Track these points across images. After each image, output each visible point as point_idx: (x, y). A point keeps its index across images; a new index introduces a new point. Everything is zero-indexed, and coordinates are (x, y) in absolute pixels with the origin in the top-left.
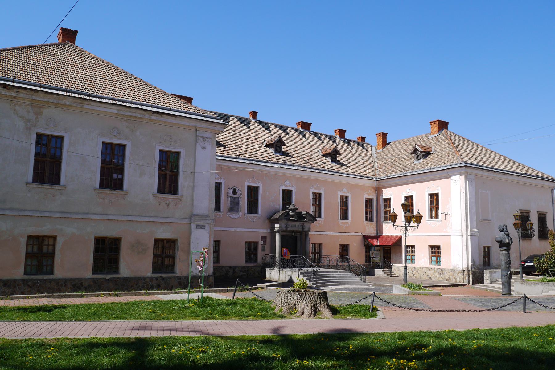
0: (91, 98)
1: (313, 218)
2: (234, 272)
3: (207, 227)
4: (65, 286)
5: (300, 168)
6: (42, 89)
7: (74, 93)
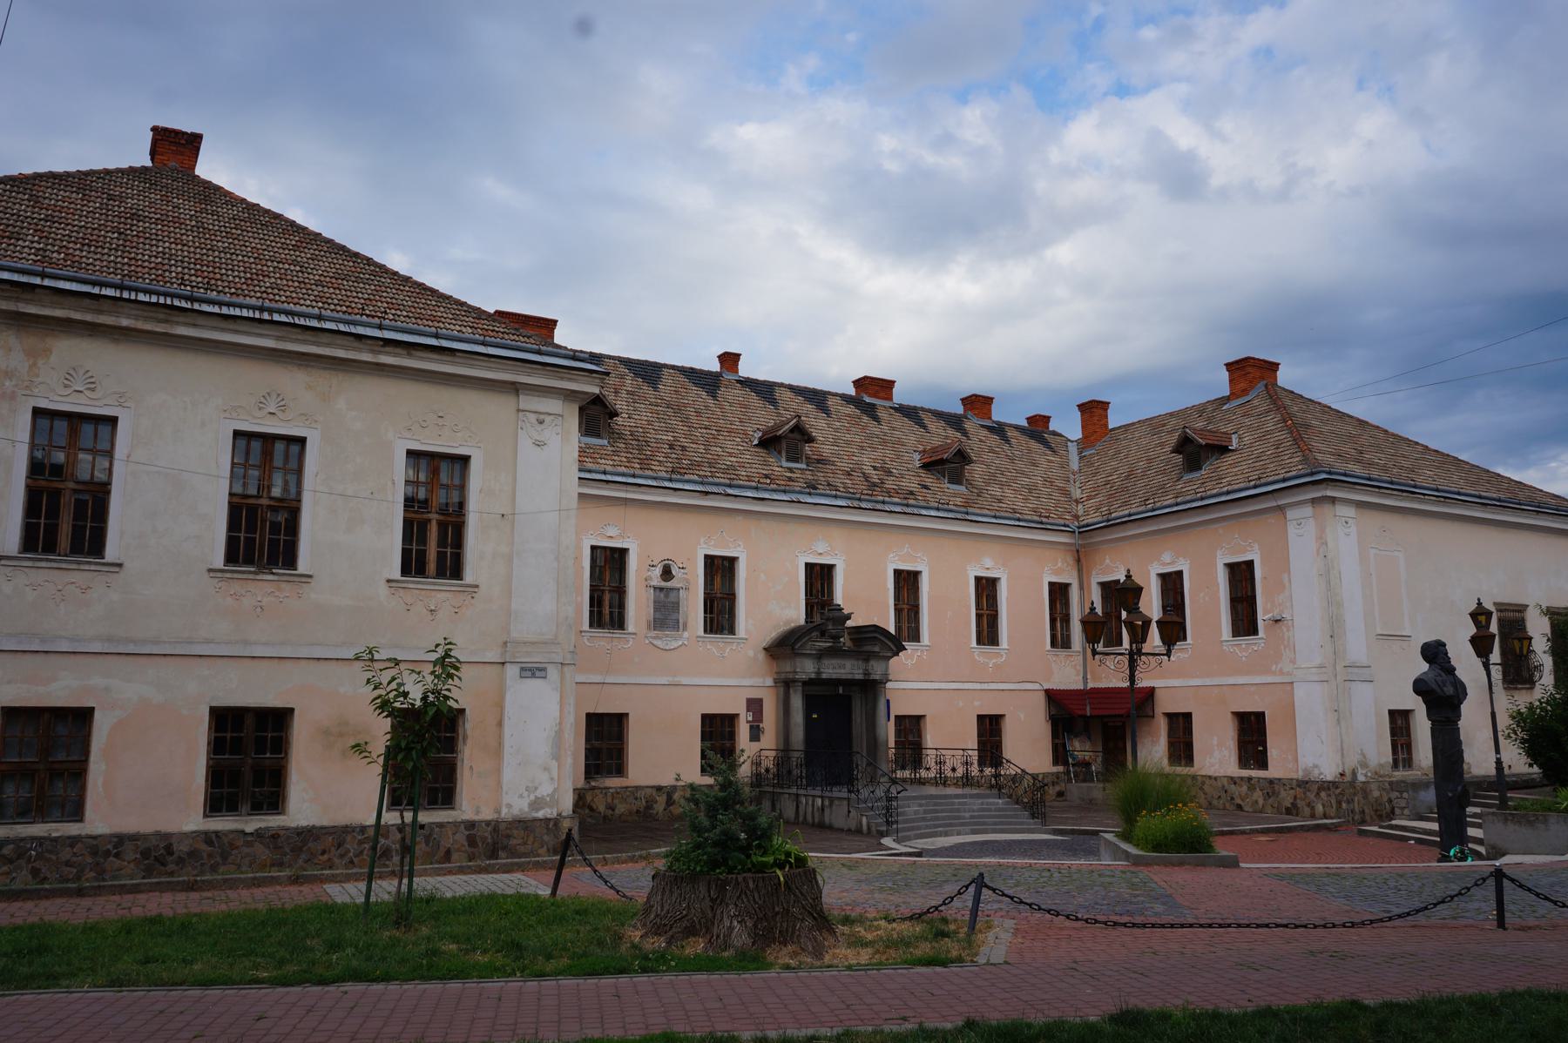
0: (196, 306)
1: (895, 644)
2: (670, 802)
3: (553, 672)
4: (117, 855)
5: (856, 504)
6: (47, 282)
7: (145, 291)
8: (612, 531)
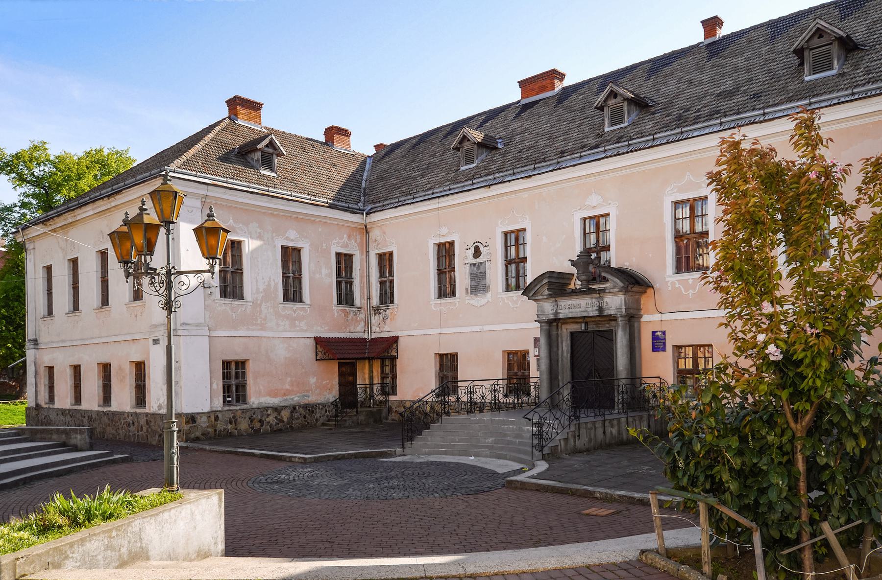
8: (444, 231)
